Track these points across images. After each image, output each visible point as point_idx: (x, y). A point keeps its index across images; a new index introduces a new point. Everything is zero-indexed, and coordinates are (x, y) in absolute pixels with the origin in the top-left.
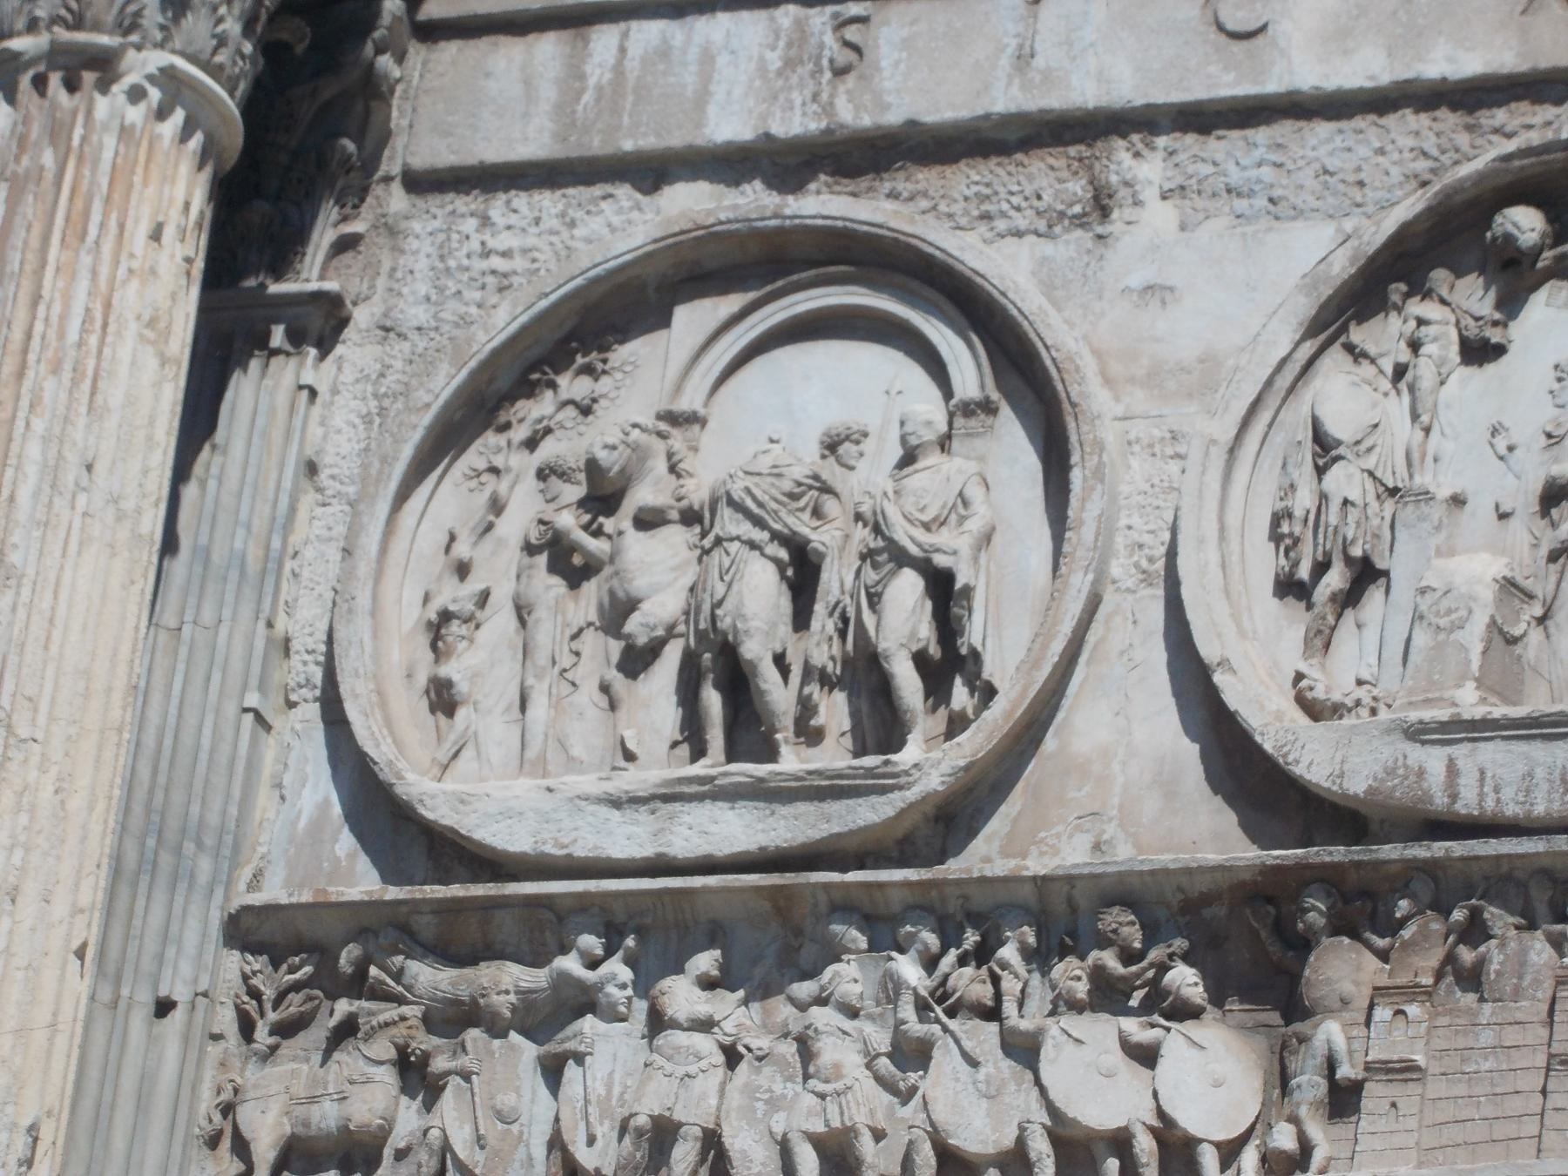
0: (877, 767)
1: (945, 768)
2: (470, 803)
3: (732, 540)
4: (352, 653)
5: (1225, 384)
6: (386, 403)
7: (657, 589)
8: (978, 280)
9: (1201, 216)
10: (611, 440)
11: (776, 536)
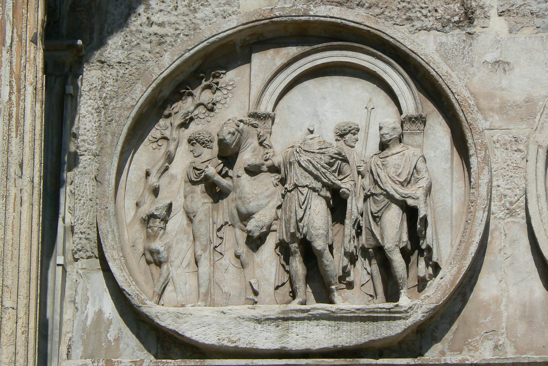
0: (392, 308)
1: (425, 308)
2: (182, 318)
3: (304, 187)
4: (110, 237)
5: (539, 114)
6: (107, 102)
7: (261, 207)
8: (414, 55)
9: (519, 26)
10: (232, 130)
11: (324, 185)
